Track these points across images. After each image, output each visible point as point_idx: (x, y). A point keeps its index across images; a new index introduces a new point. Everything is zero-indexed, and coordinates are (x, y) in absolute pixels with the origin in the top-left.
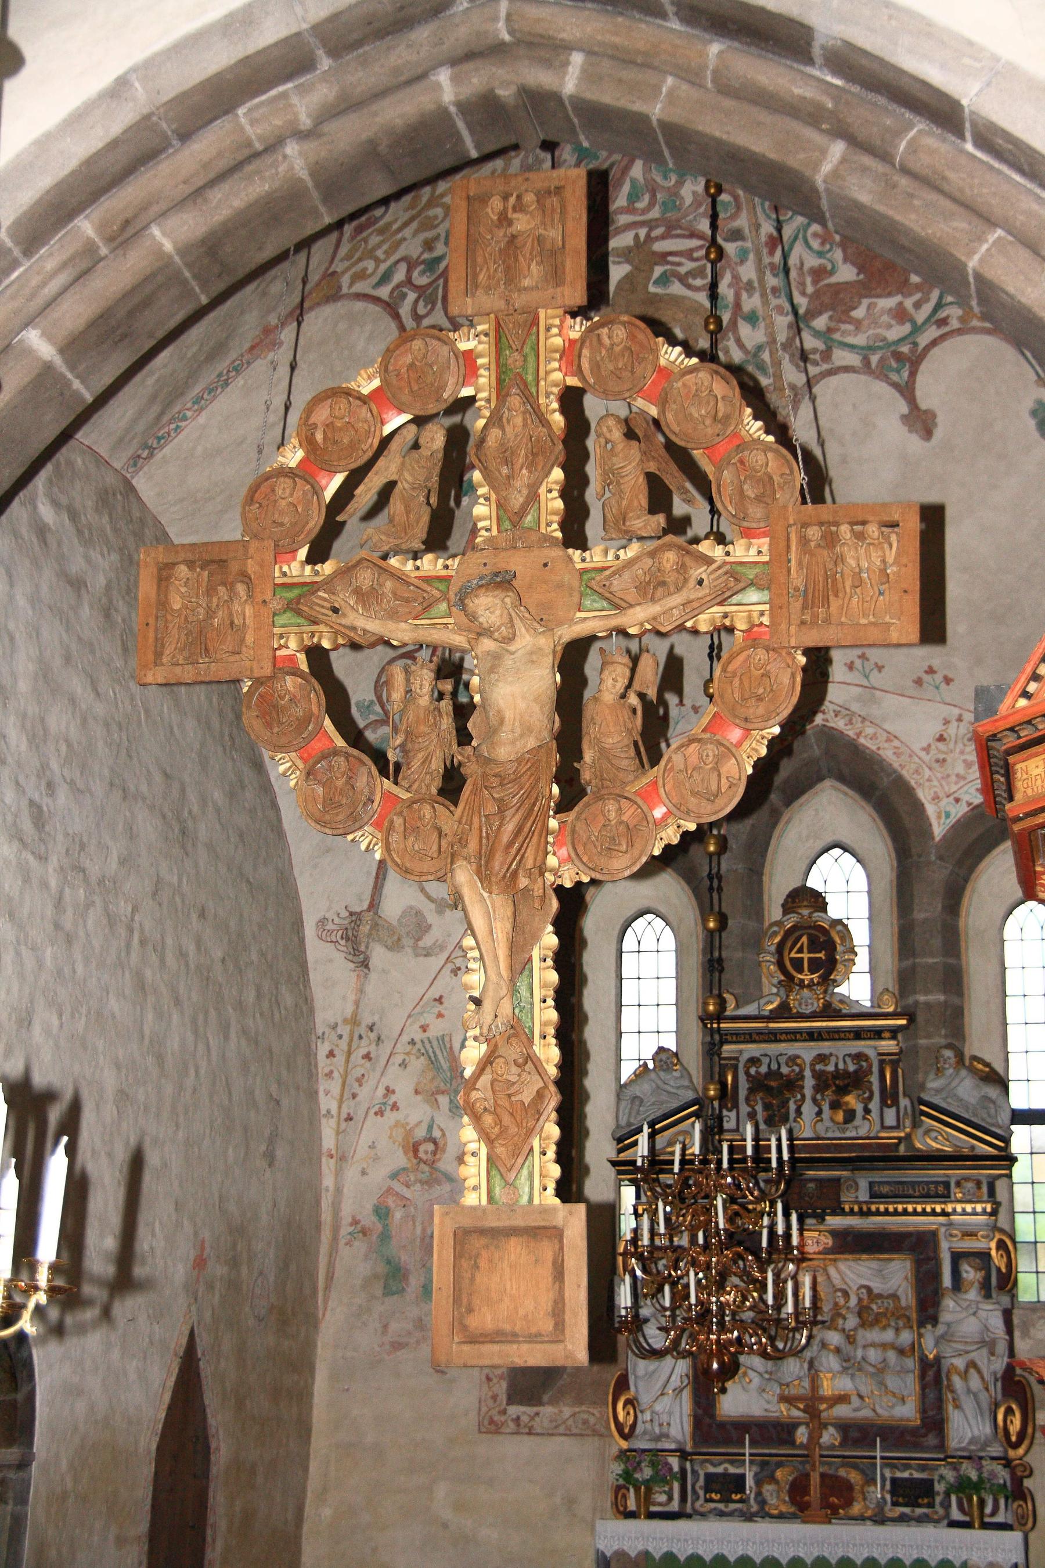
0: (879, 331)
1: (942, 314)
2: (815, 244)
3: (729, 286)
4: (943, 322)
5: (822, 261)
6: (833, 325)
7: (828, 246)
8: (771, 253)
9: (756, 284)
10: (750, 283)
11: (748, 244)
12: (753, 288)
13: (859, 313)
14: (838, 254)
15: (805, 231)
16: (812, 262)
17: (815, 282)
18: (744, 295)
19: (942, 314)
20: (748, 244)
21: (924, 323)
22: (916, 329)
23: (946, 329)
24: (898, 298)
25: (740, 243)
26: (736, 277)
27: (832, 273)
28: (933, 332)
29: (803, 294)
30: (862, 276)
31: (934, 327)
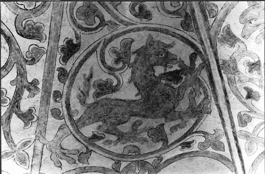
0: (136, 144)
1: (189, 139)
2: (110, 60)
3: (12, 82)
4: (188, 145)
5: (112, 77)
6: (100, 133)
7: (121, 65)
8: (65, 59)
9: (40, 86)
10: (35, 83)
11: (44, 45)
12: (36, 88)
13: (125, 128)
14: (126, 75)
15: (105, 45)
16: (102, 76)
17: (97, 95)
18: (26, 93)
19: (189, 139)
20: (44, 45)
21: (172, 144)
22: (167, 146)
23: (187, 150)
24: (163, 120)
25: (34, 42)
26: (22, 74)
27: (114, 90)
28: (178, 151)
29: (83, 102)
30: (139, 97)
31: (180, 147)
